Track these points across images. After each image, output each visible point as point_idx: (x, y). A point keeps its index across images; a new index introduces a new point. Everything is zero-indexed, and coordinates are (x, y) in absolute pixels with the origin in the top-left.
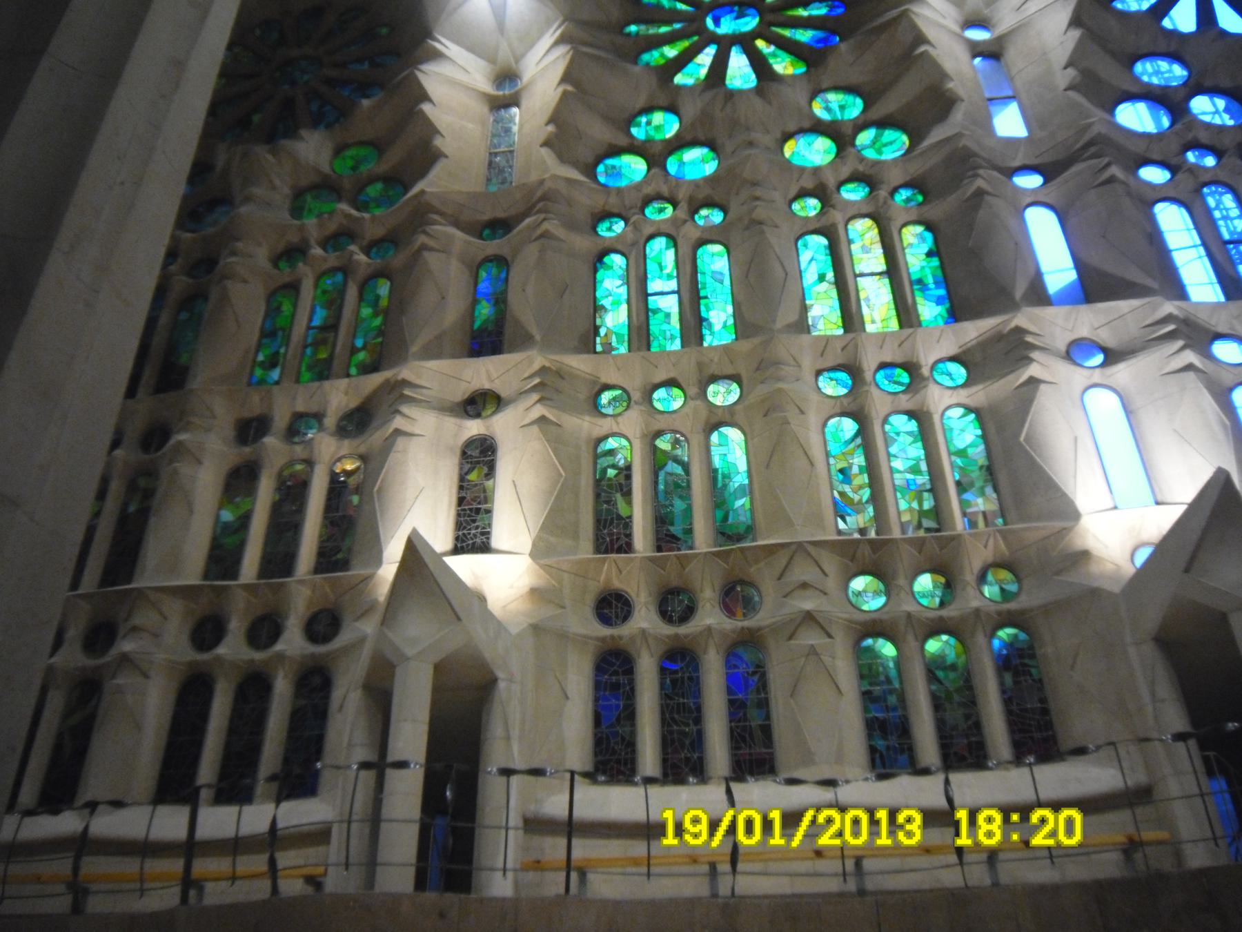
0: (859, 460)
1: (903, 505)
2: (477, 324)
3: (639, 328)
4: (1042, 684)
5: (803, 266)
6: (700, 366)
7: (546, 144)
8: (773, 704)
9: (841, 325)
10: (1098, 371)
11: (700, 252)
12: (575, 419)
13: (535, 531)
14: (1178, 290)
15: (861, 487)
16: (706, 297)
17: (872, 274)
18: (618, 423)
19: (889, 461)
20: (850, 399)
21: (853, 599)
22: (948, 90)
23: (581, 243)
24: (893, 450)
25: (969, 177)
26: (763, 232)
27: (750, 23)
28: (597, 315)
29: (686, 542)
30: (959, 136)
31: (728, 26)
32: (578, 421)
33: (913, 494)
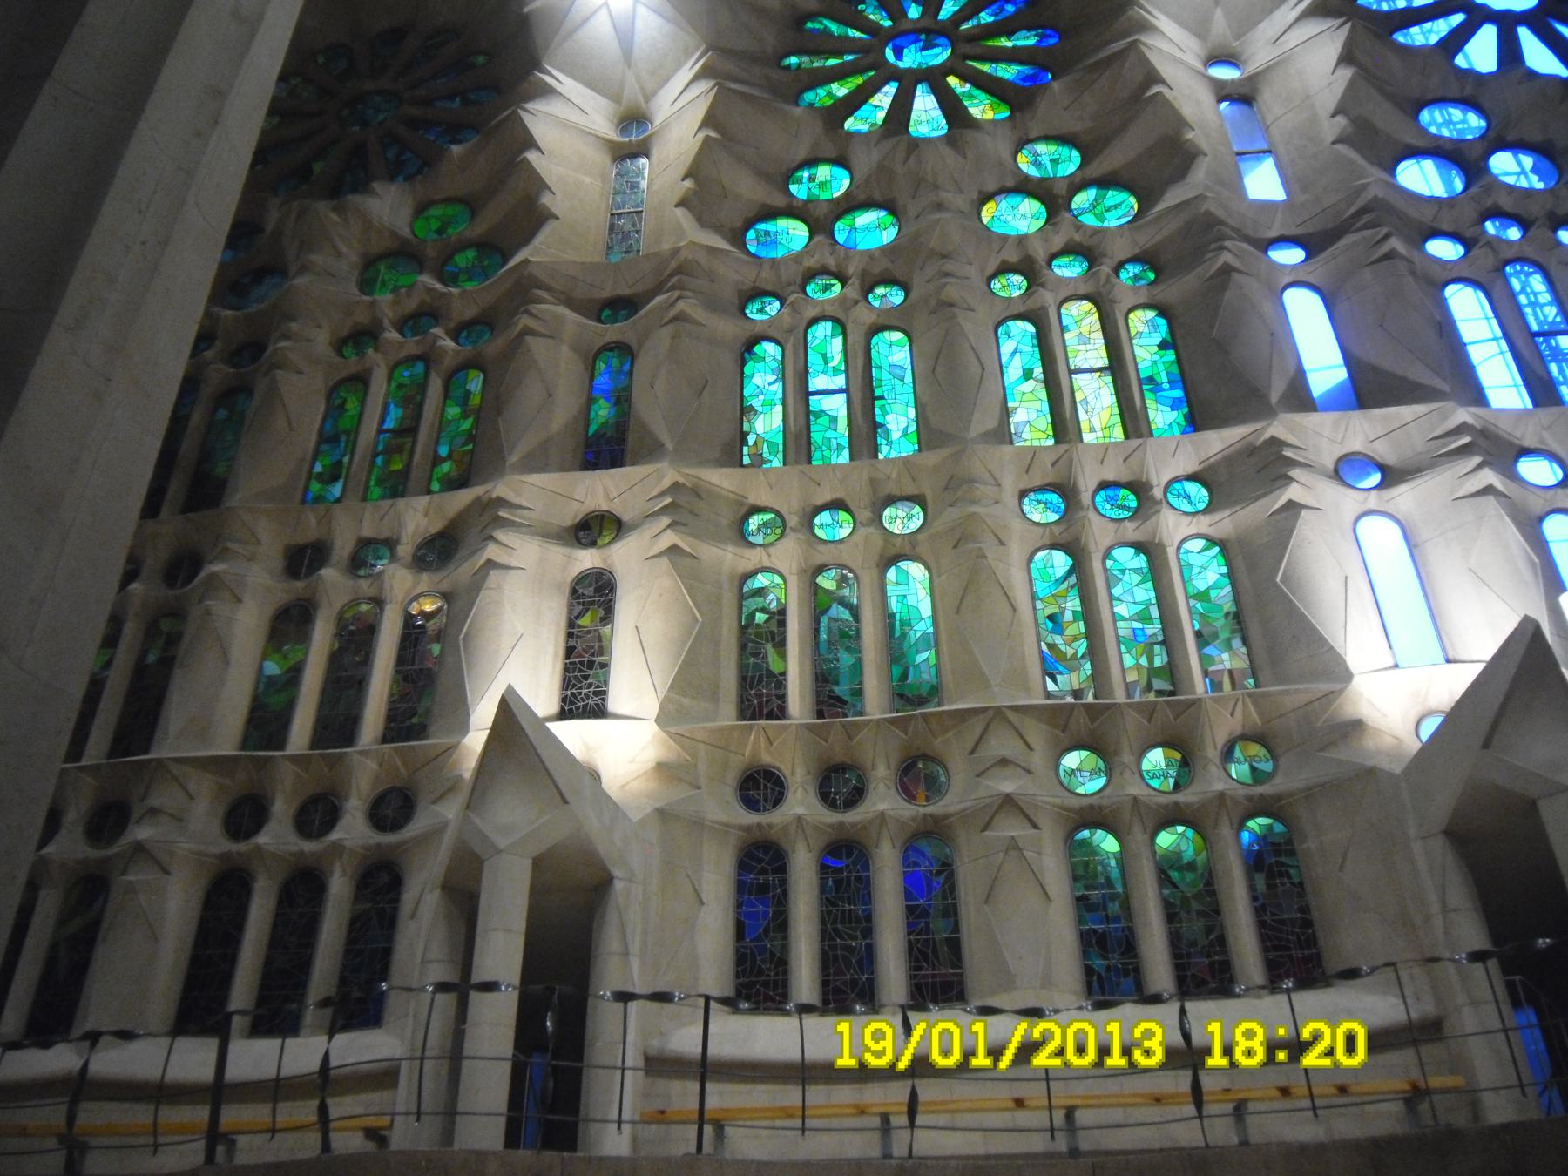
0: (1073, 604)
1: (1129, 661)
2: (593, 429)
3: (797, 437)
4: (1303, 889)
5: (1004, 360)
6: (873, 482)
7: (682, 203)
8: (962, 911)
9: (1051, 433)
10: (1374, 493)
11: (874, 340)
12: (715, 549)
13: (663, 690)
14: (1477, 396)
15: (1075, 638)
16: (882, 398)
17: (1091, 370)
18: (769, 556)
19: (1112, 606)
20: (1062, 528)
21: (1065, 780)
22: (1188, 140)
23: (727, 328)
24: (1116, 591)
25: (1212, 251)
26: (954, 316)
27: (939, 55)
29: (854, 706)
30: (1200, 198)
31: (912, 58)
32: (720, 552)
33: (1140, 648)
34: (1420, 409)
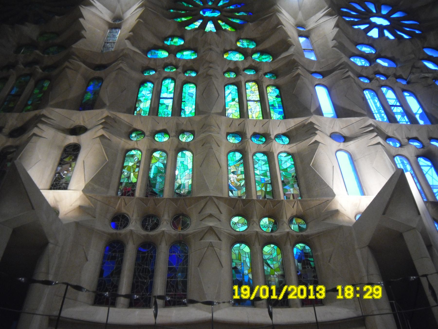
0: (241, 169)
1: (258, 188)
2: (84, 101)
3: (154, 108)
4: (315, 269)
5: (226, 95)
6: (178, 125)
7: (128, 39)
8: (189, 272)
11: (184, 86)
12: (118, 139)
13: (88, 181)
15: (241, 180)
17: (254, 101)
18: (137, 144)
19: (254, 171)
20: (240, 144)
21: (232, 226)
22: (289, 41)
23: (136, 75)
24: (256, 166)
25: (295, 69)
26: (212, 78)
27: (217, 14)
28: (137, 103)
29: (160, 195)
30: (292, 55)
31: (208, 14)
32: (120, 140)
33: (263, 184)
34: (357, 119)
